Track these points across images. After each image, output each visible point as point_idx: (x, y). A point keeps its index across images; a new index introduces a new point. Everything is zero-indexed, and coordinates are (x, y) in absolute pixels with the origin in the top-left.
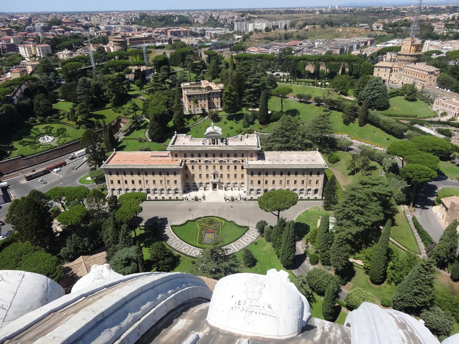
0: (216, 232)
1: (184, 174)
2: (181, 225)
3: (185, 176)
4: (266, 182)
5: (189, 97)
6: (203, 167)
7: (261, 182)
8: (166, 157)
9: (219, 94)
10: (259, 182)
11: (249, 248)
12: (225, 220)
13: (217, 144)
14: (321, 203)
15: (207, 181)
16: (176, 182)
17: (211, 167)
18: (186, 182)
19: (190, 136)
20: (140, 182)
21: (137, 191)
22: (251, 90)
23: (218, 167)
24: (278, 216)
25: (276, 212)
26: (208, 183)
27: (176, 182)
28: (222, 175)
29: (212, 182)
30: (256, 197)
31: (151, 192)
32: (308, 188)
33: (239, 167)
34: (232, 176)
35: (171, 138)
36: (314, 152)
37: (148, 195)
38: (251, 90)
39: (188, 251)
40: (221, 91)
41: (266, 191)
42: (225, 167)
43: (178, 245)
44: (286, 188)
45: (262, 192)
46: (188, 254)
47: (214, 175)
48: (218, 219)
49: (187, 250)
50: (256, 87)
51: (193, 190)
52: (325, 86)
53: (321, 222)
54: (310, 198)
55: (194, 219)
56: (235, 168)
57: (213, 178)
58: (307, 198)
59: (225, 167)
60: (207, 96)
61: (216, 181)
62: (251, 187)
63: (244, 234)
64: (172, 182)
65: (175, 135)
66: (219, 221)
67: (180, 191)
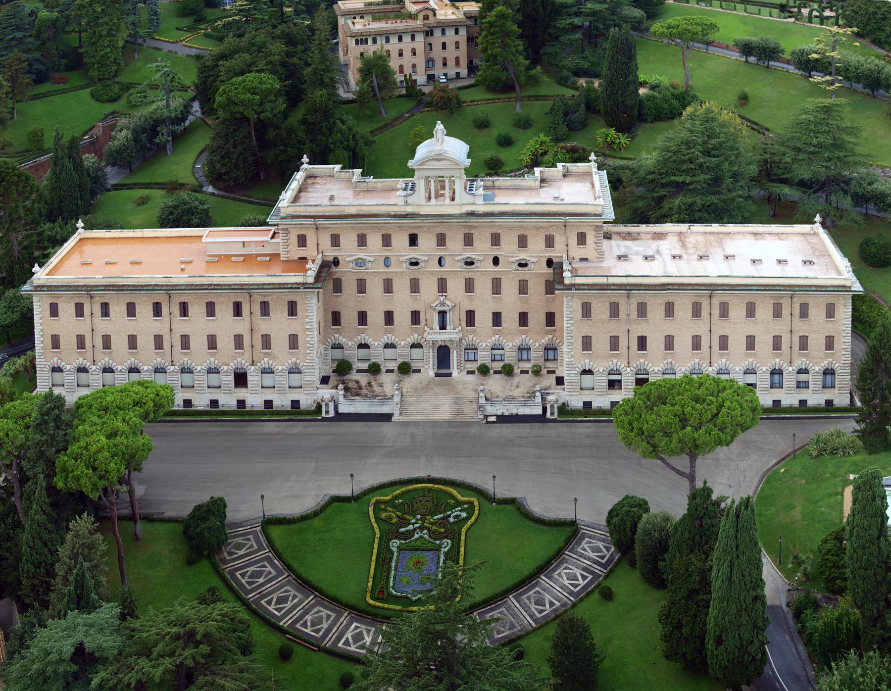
0: (446, 545)
1: (325, 311)
2: (304, 518)
4: (642, 343)
5: (361, 40)
6: (401, 287)
7: (623, 343)
9: (463, 32)
10: (614, 343)
11: (578, 613)
12: (479, 492)
14: (849, 427)
15: (414, 338)
16: (293, 343)
17: (429, 288)
18: (331, 340)
20: (159, 342)
21: (143, 377)
22: (577, 21)
23: (456, 286)
24: (692, 478)
25: (682, 462)
26: (415, 346)
27: (293, 343)
29: (434, 342)
30: (602, 400)
32: (800, 363)
33: (536, 288)
35: (284, 181)
36: (805, 228)
38: (577, 21)
39: (329, 630)
40: (469, 23)
42: (483, 287)
43: (289, 605)
44: (716, 367)
45: (628, 379)
46: (328, 643)
47: (442, 314)
48: (454, 492)
49: (325, 625)
50: (594, 13)
51: (359, 371)
52: (823, 20)
53: (855, 501)
54: (810, 403)
55: (357, 490)
56: (523, 288)
58: (796, 403)
59: (483, 287)
60: (420, 38)
61: (449, 335)
62: (587, 364)
63: (559, 553)
64: (280, 342)
66: (459, 497)
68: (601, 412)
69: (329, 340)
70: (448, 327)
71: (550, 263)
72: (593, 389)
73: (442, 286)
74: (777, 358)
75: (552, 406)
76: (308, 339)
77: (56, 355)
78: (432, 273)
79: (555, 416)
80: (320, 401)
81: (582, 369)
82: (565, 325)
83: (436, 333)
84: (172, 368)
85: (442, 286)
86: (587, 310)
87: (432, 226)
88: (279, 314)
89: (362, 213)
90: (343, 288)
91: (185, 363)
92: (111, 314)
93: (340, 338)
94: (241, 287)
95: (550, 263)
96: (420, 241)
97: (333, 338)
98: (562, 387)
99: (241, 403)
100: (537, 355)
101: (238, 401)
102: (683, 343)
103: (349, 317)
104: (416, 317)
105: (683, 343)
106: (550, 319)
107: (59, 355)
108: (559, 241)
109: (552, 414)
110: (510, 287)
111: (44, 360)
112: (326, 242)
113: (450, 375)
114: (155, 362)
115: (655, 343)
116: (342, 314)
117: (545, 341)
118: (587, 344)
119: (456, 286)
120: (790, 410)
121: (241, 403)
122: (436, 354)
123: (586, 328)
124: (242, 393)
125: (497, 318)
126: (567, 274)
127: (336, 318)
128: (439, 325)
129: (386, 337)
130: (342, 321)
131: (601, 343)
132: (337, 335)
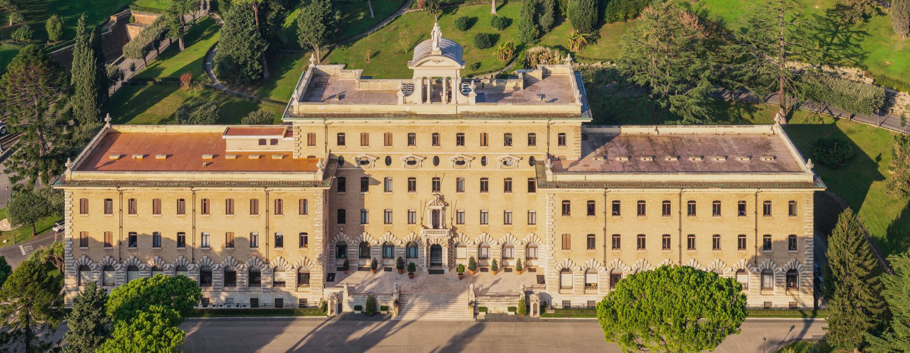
3: (335, 215)
4: (616, 242)
7: (599, 242)
8: (274, 142)
10: (591, 242)
13: (449, 101)
16: (303, 240)
18: (337, 239)
19: (358, 72)
27: (303, 240)
28: (460, 216)
30: (579, 300)
31: (218, 277)
34: (495, 219)
37: (207, 293)
41: (614, 278)
45: (601, 278)
47: (435, 213)
56: (508, 186)
57: (430, 226)
59: (471, 186)
65: (312, 65)
67: (317, 274)
68: (580, 311)
69: (335, 238)
70: (441, 227)
71: (532, 161)
72: (572, 287)
73: (436, 185)
74: (742, 258)
75: (535, 305)
76: (316, 238)
77: (84, 252)
78: (428, 173)
79: (538, 315)
80: (325, 299)
81: (562, 268)
82: (547, 223)
83: (430, 232)
84: (192, 266)
85: (436, 185)
86: (566, 208)
87: (427, 127)
88: (291, 210)
89: (365, 113)
90: (347, 187)
91: (205, 260)
92: (138, 211)
93: (345, 236)
94: (259, 184)
95: (532, 161)
96: (418, 140)
97: (338, 236)
98: (543, 286)
99: (254, 302)
100: (518, 253)
101: (252, 299)
102: (654, 242)
103: (352, 215)
104: (411, 215)
105: (654, 242)
106: (531, 218)
107: (87, 253)
108: (541, 139)
109: (535, 312)
110: (496, 186)
111: (72, 258)
112: (333, 140)
113: (442, 272)
114: (177, 260)
115: (629, 242)
116: (347, 211)
117: (526, 240)
118: (566, 243)
119: (448, 188)
120: (757, 311)
121: (254, 302)
122: (429, 253)
123: (565, 225)
124: (255, 292)
125: (483, 217)
126: (549, 173)
127: (341, 216)
128: (433, 224)
129: (384, 236)
130: (347, 218)
131: (579, 242)
132: (342, 233)
